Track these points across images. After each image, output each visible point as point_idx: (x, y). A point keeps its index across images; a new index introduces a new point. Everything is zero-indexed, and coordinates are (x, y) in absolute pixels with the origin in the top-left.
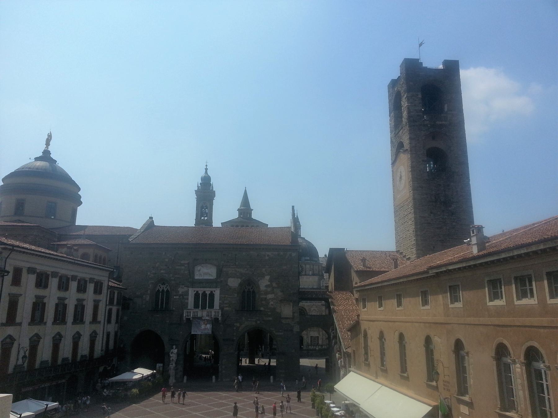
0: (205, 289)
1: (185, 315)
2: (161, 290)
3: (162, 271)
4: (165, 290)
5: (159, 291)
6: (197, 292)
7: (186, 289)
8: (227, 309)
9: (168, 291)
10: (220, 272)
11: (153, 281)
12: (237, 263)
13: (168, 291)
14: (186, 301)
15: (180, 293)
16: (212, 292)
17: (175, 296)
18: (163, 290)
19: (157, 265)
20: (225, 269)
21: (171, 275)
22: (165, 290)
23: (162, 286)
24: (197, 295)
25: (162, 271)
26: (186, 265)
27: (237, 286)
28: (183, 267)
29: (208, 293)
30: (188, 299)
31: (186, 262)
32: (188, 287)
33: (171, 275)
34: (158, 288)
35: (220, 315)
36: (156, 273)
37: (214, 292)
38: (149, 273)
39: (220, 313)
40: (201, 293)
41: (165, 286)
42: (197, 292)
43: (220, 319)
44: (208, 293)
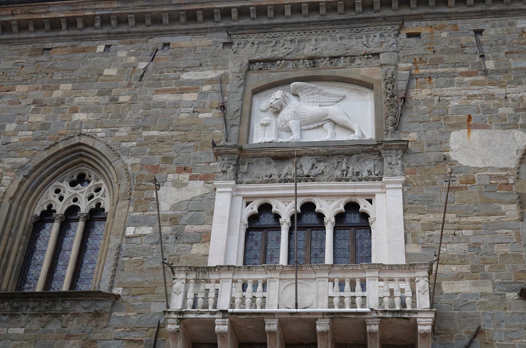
0: (307, 189)
1: (176, 303)
2: (60, 208)
3: (80, 116)
4: (84, 206)
5: (48, 214)
6: (265, 208)
7: (198, 188)
8: (464, 287)
9: (97, 214)
10: (395, 105)
11: (24, 160)
12: (490, 65)
13: (97, 214)
14: (197, 249)
15: (165, 207)
16: (352, 207)
17: (136, 223)
18: (73, 210)
19: (57, 94)
20: (420, 94)
21: (123, 132)
22: (84, 206)
23: (68, 191)
24: (260, 223)
25: (80, 116)
26: (206, 88)
27: (512, 164)
28: (190, 97)
29: (329, 209)
30: (205, 238)
31: (211, 74)
32: (207, 178)
33: (123, 132)
34: (49, 196)
35: (424, 301)
36: (44, 126)
37: (364, 206)
38: (10, 127)
39: (422, 284)
40: (285, 210)
41: (82, 192)
42: (265, 208)
43: (424, 325)
44: (329, 209)
